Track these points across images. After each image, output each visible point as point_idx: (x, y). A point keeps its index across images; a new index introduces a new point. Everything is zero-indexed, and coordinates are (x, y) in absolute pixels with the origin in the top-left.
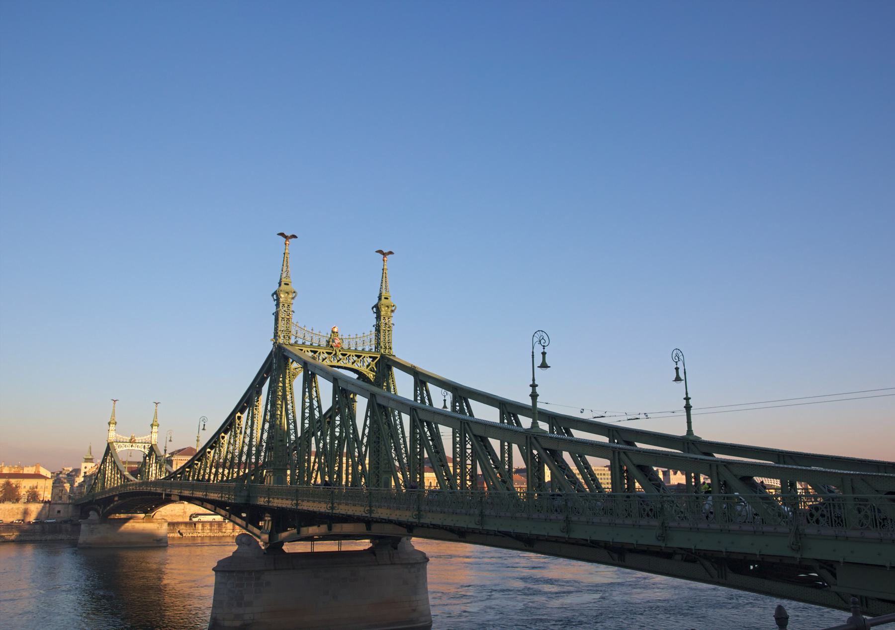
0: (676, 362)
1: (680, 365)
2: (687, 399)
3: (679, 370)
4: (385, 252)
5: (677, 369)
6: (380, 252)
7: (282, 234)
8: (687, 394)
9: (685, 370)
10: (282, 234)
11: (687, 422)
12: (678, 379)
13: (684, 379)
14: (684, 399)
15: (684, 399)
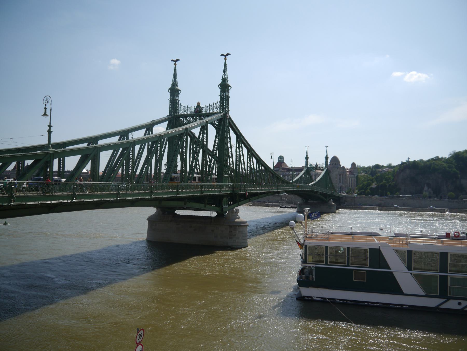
0: (46, 104)
1: (48, 107)
2: (50, 126)
3: (47, 110)
4: (224, 54)
5: (46, 109)
6: (222, 55)
7: (172, 61)
8: (50, 123)
9: (51, 108)
10: (172, 61)
11: (48, 141)
12: (45, 115)
13: (49, 115)
14: (48, 126)
15: (48, 126)
